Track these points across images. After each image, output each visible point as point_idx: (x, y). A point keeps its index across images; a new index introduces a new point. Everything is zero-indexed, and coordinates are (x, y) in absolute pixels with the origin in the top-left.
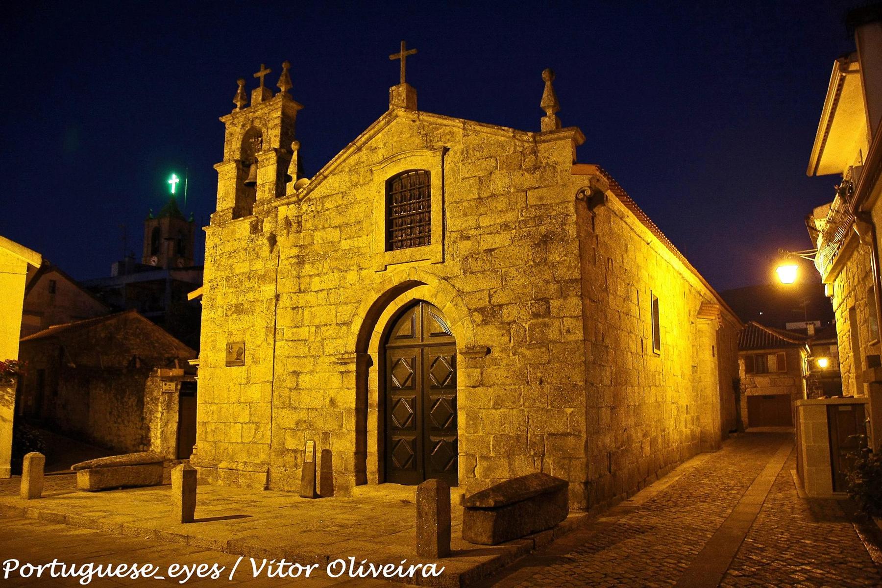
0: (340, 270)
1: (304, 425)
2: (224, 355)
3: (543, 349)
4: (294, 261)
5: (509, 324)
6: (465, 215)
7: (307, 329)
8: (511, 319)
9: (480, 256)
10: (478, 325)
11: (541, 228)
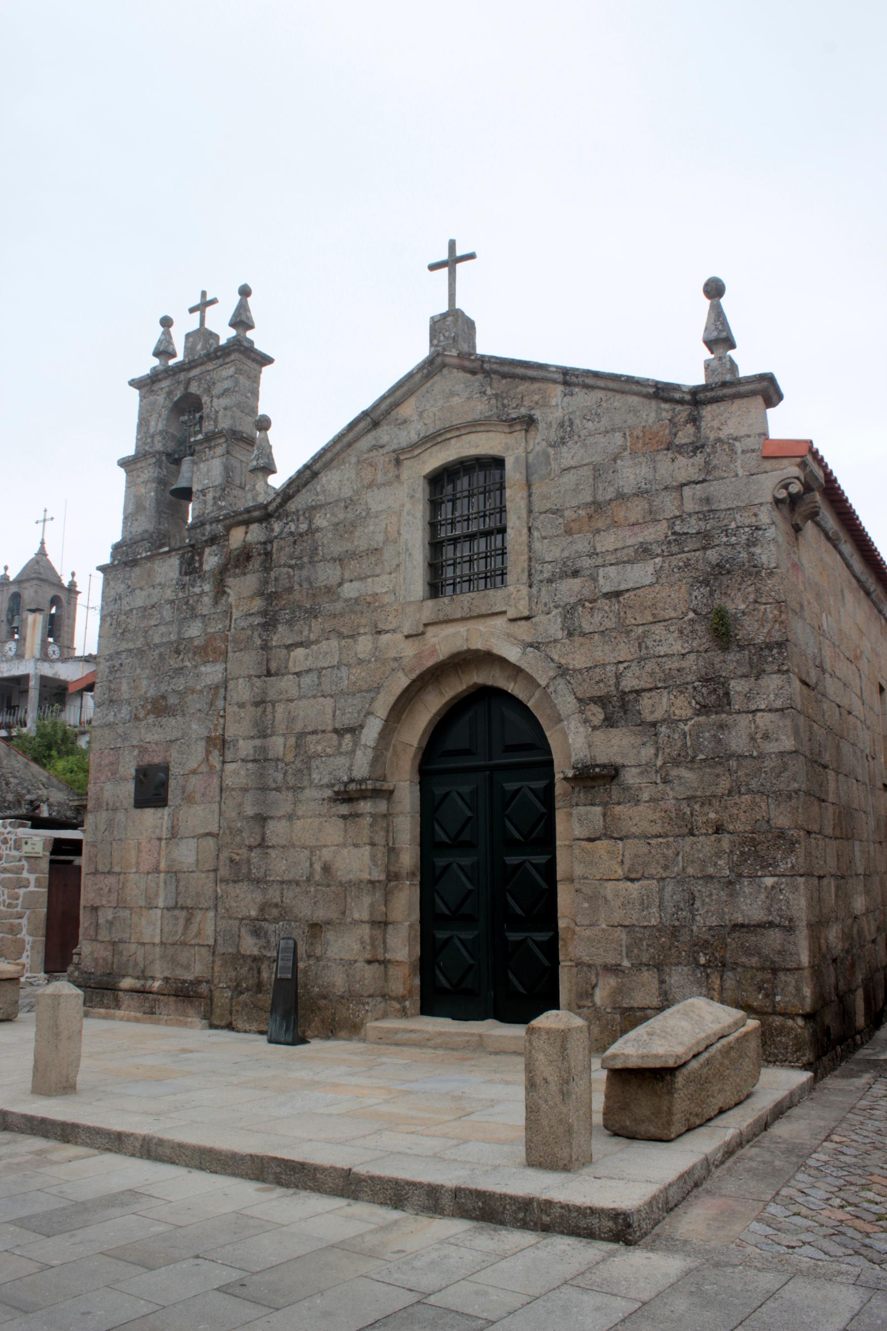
0: (341, 636)
1: (275, 912)
2: (131, 787)
3: (719, 770)
4: (258, 620)
5: (654, 724)
6: (569, 532)
8: (658, 715)
9: (599, 604)
10: (594, 728)
11: (709, 552)
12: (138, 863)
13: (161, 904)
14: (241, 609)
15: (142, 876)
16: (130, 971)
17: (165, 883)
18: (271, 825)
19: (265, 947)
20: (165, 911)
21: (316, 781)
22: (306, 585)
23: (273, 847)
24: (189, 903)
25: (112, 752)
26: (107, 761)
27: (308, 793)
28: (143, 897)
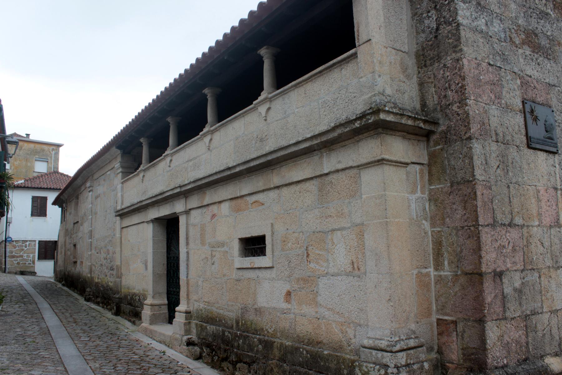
12: (539, 214)
16: (548, 350)
28: (549, 255)
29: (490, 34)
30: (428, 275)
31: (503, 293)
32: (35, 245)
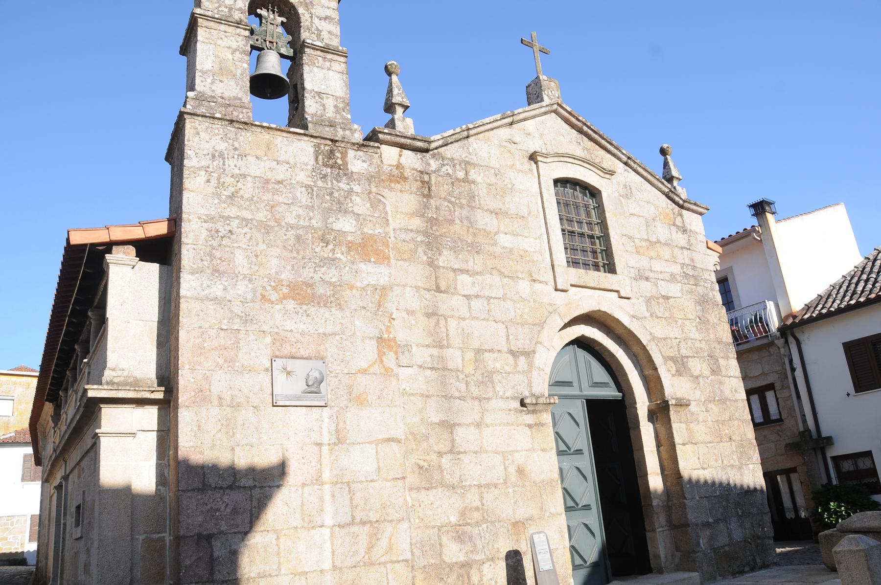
1: (477, 515)
7: (458, 353)
13: (329, 521)
14: (398, 221)
15: (293, 489)
17: (333, 496)
18: (459, 432)
19: (472, 552)
20: (337, 529)
21: (501, 393)
22: (466, 223)
23: (465, 452)
24: (373, 517)
25: (222, 334)
26: (215, 343)
27: (494, 404)
28: (298, 515)
29: (228, 298)
30: (162, 539)
31: (212, 556)
32: (25, 521)
